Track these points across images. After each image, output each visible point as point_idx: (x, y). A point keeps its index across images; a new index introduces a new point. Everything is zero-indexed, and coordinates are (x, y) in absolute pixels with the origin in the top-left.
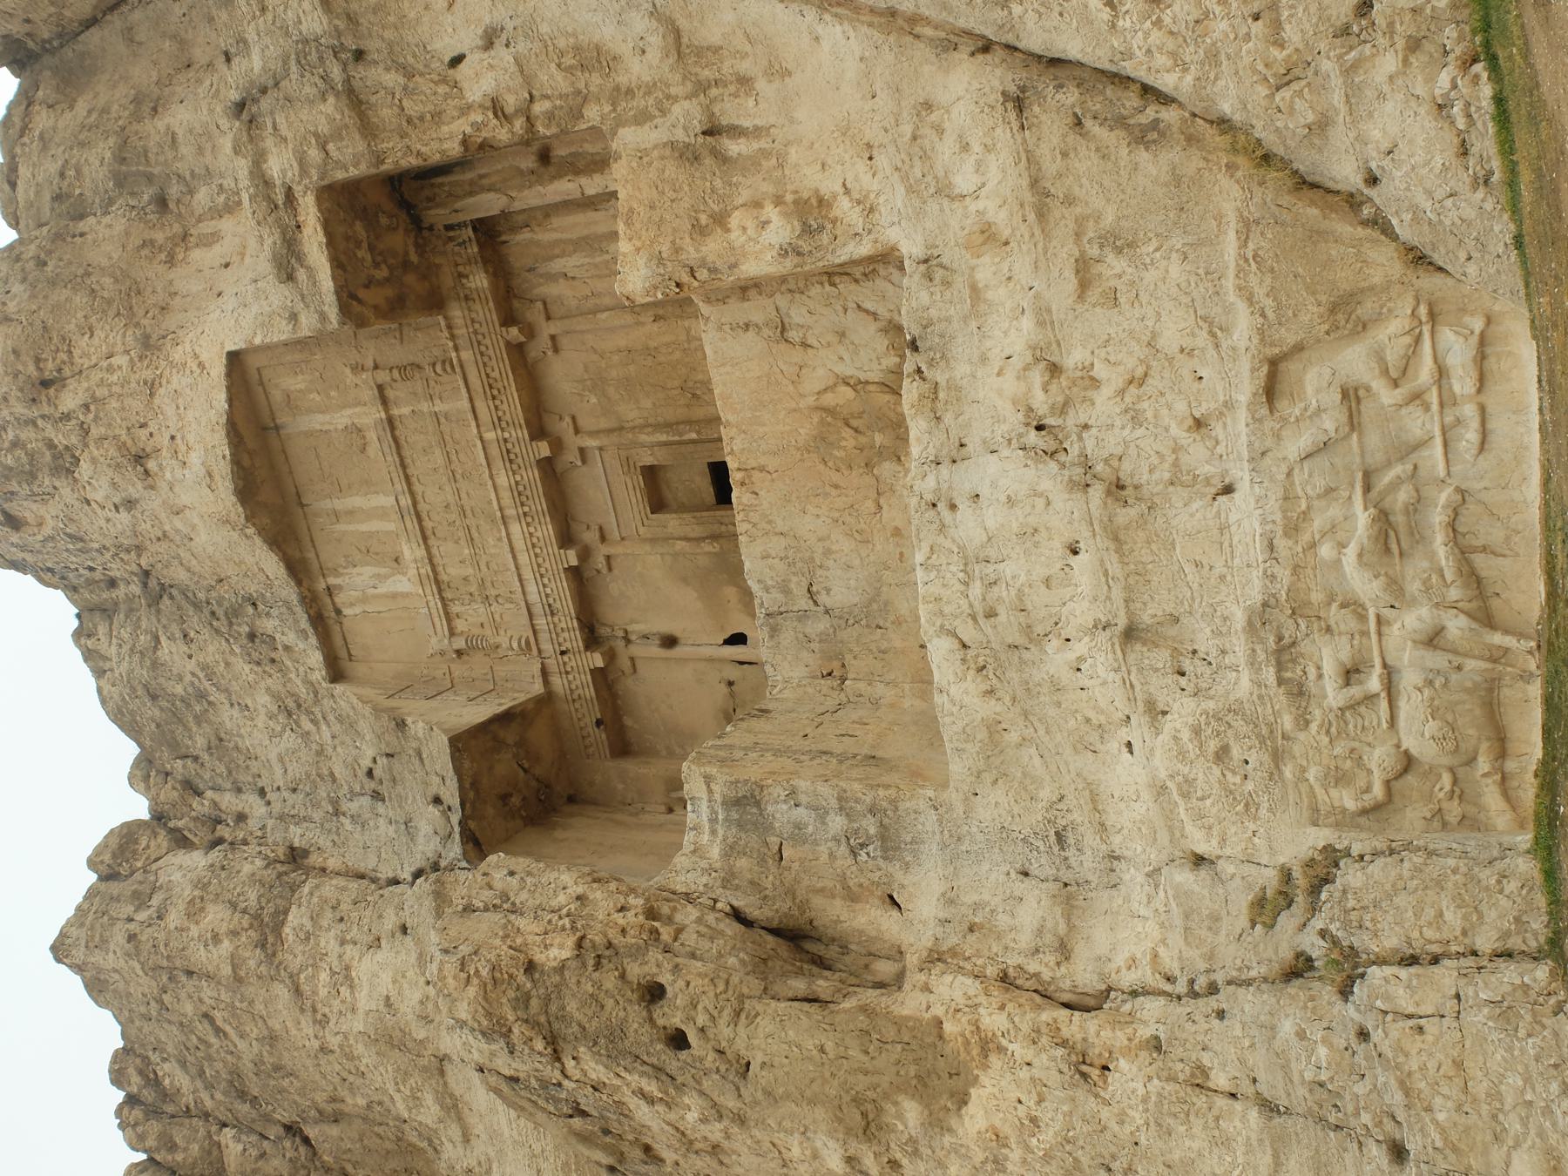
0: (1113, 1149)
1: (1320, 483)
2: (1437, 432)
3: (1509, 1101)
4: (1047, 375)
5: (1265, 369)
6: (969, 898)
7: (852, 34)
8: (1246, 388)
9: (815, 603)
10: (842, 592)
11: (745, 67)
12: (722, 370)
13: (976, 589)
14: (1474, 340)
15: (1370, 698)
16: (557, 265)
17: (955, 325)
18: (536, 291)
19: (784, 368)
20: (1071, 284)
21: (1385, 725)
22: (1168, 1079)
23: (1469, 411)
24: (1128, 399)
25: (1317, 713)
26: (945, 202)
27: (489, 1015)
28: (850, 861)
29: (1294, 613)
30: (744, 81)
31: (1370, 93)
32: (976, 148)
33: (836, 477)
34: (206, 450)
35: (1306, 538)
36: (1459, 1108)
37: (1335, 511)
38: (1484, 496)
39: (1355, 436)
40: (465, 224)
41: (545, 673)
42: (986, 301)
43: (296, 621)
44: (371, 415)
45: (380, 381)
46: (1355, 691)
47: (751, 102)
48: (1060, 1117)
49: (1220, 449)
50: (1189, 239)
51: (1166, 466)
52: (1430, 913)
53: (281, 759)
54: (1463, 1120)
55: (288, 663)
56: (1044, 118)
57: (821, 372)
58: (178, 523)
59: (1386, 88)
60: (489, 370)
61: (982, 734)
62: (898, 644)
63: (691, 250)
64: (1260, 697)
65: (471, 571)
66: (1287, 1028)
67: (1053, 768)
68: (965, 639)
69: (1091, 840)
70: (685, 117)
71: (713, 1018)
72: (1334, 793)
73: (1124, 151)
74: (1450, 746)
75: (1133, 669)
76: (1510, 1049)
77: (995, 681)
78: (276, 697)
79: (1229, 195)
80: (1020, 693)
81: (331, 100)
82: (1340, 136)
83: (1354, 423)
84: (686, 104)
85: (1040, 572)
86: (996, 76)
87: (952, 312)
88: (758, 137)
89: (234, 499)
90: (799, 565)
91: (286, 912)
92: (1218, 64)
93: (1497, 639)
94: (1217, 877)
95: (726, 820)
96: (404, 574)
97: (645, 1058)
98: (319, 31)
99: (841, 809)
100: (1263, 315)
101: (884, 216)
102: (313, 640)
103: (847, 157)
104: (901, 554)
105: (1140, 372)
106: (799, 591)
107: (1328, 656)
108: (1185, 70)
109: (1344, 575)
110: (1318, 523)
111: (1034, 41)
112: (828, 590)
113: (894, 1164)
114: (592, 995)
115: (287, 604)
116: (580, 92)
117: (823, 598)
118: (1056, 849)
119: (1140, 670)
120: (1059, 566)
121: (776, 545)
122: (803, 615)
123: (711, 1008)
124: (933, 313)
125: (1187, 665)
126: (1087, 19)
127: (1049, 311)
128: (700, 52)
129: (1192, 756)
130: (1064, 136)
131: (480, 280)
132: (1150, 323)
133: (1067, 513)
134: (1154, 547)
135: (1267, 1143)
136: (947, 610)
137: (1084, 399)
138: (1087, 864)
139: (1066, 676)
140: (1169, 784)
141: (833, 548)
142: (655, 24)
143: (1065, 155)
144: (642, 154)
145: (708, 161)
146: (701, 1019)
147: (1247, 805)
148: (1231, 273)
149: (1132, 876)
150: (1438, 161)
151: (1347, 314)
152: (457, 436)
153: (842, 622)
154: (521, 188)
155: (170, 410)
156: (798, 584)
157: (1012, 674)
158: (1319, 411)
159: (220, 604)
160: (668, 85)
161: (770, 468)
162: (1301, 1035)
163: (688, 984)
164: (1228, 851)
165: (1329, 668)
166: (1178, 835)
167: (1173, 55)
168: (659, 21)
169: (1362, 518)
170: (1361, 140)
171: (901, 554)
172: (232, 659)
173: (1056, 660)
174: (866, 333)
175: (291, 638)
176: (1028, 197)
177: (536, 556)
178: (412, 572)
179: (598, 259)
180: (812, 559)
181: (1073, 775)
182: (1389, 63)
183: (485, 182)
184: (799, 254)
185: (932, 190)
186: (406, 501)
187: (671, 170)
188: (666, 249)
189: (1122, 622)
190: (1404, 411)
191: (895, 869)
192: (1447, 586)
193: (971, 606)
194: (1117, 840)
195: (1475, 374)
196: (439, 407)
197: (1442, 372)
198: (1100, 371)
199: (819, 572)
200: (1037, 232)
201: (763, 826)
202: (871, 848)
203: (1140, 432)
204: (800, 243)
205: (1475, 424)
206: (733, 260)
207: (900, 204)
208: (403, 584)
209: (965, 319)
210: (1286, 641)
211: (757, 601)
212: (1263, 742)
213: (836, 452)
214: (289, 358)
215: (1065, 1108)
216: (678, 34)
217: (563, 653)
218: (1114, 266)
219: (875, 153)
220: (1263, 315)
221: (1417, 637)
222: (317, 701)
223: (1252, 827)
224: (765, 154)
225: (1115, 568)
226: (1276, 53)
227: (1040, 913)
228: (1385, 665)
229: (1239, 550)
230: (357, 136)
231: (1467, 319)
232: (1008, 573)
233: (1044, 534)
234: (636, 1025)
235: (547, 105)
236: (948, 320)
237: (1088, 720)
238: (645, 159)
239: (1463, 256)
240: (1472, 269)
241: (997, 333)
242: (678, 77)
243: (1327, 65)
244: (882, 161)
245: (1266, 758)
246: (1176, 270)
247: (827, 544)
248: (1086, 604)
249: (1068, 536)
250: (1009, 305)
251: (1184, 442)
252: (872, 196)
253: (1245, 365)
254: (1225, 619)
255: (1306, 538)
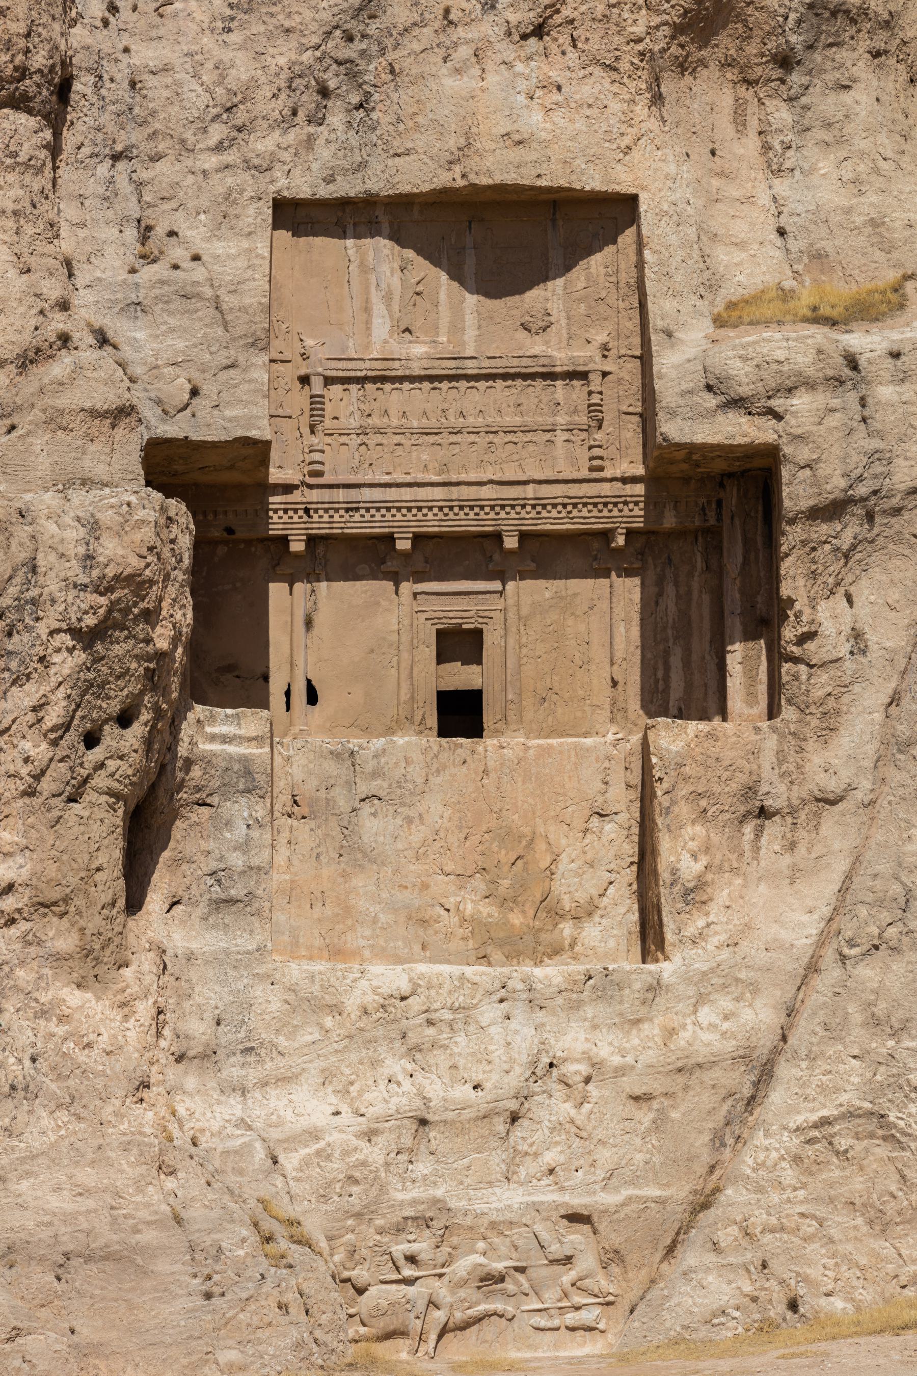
0: (92, 1107)
1: (520, 1243)
2: (546, 1306)
3: (260, 1348)
4: (585, 1074)
5: (586, 1213)
6: (193, 975)
7: (809, 941)
8: (577, 1202)
9: (363, 800)
10: (373, 826)
11: (801, 849)
12: (573, 753)
13: (448, 1015)
14: (593, 1325)
15: (398, 1269)
16: (670, 590)
17: (618, 1007)
18: (650, 560)
19: (570, 809)
20: (638, 1092)
21: (382, 1278)
22: (160, 1149)
23: (556, 1322)
24: (567, 1126)
25: (386, 1239)
26: (693, 1000)
27: (117, 578)
28: (206, 870)
29: (447, 1227)
30: (792, 846)
31: (732, 1276)
32: (726, 1026)
33: (474, 839)
34: (546, 144)
35: (489, 1234)
36: (249, 1325)
37: (503, 1250)
38: (510, 1329)
39: (546, 1262)
40: (719, 519)
41: (288, 488)
42: (631, 1029)
43: (345, 171)
44: (557, 351)
45: (591, 376)
46: (401, 1262)
47: (777, 848)
48: (101, 1068)
49: (535, 1181)
50: (657, 1167)
51: (526, 1148)
52: (323, 1308)
53: (166, 69)
54: (244, 1327)
55: (291, 137)
56: (737, 1073)
57: (564, 841)
58: (464, 52)
59: (734, 1285)
60: (590, 507)
61: (329, 1000)
62: (325, 872)
63: (684, 792)
64: (393, 1206)
65: (395, 422)
66: (245, 1233)
67: (306, 1051)
68: (410, 1001)
69: (253, 1075)
70: (778, 794)
71: (112, 775)
72: (342, 1249)
73: (711, 1125)
74: (374, 1313)
75: (398, 1123)
76: (285, 1348)
77: (375, 1017)
78: (246, 94)
79: (680, 1192)
80: (368, 1035)
81: (843, 483)
82: (711, 1258)
83: (553, 1262)
84: (785, 796)
85: (461, 1062)
86: (766, 1042)
87: (626, 1005)
88: (753, 851)
89: (498, 179)
90: (399, 792)
91: (30, 112)
92: (756, 1192)
93: (433, 1337)
94: (268, 1174)
95: (230, 755)
96: (391, 333)
97: (79, 713)
98: (895, 479)
99: (251, 868)
100: (616, 1212)
101: (691, 952)
102: (324, 192)
103: (731, 927)
104: (406, 887)
105: (584, 1134)
106: (374, 786)
107: (422, 1246)
108: (755, 1170)
109: (467, 1255)
110: (496, 1240)
111: (785, 1071)
112: (374, 815)
113: (12, 921)
114: (128, 669)
115: (362, 166)
116: (807, 707)
117: (367, 808)
118: (241, 1047)
119: (399, 1127)
120: (465, 1076)
121: (416, 773)
122: (350, 784)
123: (120, 772)
124: (627, 992)
125: (403, 1157)
126: (793, 1110)
127: (623, 1075)
128: (817, 815)
129: (348, 1160)
130: (725, 1087)
131: (670, 521)
132: (611, 1141)
133: (503, 1082)
134: (479, 1140)
135: (157, 1217)
136: (433, 992)
137: (569, 1097)
138: (233, 1070)
139: (386, 1071)
140: (322, 1144)
141: (413, 826)
142: (843, 786)
143: (714, 1086)
144: (755, 753)
145: (742, 809)
146: (112, 764)
147: (324, 1196)
148: (637, 1192)
149: (234, 1107)
150: (696, 1310)
151: (613, 1258)
152: (531, 447)
153: (345, 824)
154: (742, 592)
155: (586, 91)
156: (381, 787)
157: (381, 1031)
158: (561, 1242)
159: (363, 53)
160: (800, 784)
161: (485, 781)
162: (244, 1240)
163: (136, 751)
164: (291, 1183)
165: (415, 1247)
166: (286, 1145)
167: (763, 1164)
168: (845, 790)
169: (499, 1266)
170: (708, 1270)
171: (406, 887)
172: (294, 39)
173: (396, 1066)
174: (591, 886)
175: (324, 154)
176: (692, 1061)
177: (409, 509)
178: (396, 348)
179: (670, 632)
180: (403, 804)
181: (305, 1066)
182: (748, 1288)
183: (752, 556)
184: (672, 884)
185: (702, 990)
186: (471, 367)
187: (742, 779)
188: (687, 770)
189: (430, 1117)
190: (558, 1288)
191: (202, 909)
192: (463, 1311)
193: (436, 1010)
194: (258, 1095)
195: (576, 1325)
196: (561, 437)
197: (578, 1308)
198: (587, 1107)
199: (391, 810)
200: (670, 1067)
201: (226, 790)
202: (216, 888)
203: (546, 1131)
204: (679, 886)
205: (549, 1324)
206: (673, 828)
207: (697, 966)
208: (381, 328)
209: (621, 1014)
210: (430, 1223)
211: (363, 741)
212: (366, 1207)
213: (496, 843)
214: (623, 266)
215: (108, 1072)
216: (833, 803)
217: (307, 511)
218: (645, 1117)
219: (731, 948)
220: (616, 1212)
221: (434, 1295)
222: (248, 165)
223: (313, 1200)
224: (742, 855)
225: (467, 1114)
226: (759, 1229)
227: (197, 1034)
228: (418, 1278)
229: (479, 1194)
230: (811, 503)
231: (604, 1321)
232: (459, 1039)
233: (487, 1068)
234: (104, 705)
235: (804, 677)
236: (621, 1002)
237: (352, 1083)
238: (751, 757)
239: (644, 1320)
240: (636, 1324)
241: (611, 1037)
242: (805, 795)
243: (749, 1255)
244: (725, 954)
245: (357, 1209)
246: (639, 1157)
247: (417, 820)
248: (442, 1094)
249: (488, 1085)
250: (627, 1045)
251: (540, 1160)
252: (703, 944)
253: (586, 1200)
254: (435, 1183)
255: (489, 1234)
